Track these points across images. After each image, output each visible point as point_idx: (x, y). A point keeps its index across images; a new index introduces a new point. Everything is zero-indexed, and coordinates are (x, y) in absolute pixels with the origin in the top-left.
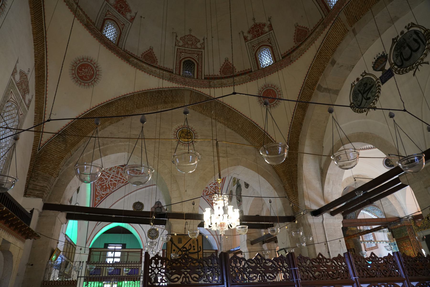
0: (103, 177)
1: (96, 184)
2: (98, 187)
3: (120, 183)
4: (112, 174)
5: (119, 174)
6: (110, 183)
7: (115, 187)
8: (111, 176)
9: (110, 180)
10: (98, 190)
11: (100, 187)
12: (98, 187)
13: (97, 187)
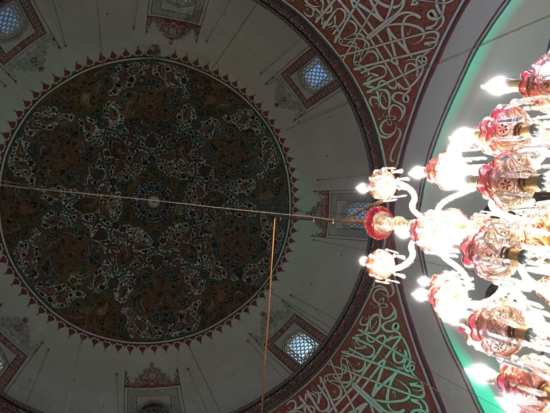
0: (404, 47)
1: (438, 34)
4: (370, 36)
5: (345, 22)
6: (391, 7)
8: (376, 32)
9: (384, 17)
10: (444, 7)
11: (431, 15)
12: (436, 19)
13: (441, 20)
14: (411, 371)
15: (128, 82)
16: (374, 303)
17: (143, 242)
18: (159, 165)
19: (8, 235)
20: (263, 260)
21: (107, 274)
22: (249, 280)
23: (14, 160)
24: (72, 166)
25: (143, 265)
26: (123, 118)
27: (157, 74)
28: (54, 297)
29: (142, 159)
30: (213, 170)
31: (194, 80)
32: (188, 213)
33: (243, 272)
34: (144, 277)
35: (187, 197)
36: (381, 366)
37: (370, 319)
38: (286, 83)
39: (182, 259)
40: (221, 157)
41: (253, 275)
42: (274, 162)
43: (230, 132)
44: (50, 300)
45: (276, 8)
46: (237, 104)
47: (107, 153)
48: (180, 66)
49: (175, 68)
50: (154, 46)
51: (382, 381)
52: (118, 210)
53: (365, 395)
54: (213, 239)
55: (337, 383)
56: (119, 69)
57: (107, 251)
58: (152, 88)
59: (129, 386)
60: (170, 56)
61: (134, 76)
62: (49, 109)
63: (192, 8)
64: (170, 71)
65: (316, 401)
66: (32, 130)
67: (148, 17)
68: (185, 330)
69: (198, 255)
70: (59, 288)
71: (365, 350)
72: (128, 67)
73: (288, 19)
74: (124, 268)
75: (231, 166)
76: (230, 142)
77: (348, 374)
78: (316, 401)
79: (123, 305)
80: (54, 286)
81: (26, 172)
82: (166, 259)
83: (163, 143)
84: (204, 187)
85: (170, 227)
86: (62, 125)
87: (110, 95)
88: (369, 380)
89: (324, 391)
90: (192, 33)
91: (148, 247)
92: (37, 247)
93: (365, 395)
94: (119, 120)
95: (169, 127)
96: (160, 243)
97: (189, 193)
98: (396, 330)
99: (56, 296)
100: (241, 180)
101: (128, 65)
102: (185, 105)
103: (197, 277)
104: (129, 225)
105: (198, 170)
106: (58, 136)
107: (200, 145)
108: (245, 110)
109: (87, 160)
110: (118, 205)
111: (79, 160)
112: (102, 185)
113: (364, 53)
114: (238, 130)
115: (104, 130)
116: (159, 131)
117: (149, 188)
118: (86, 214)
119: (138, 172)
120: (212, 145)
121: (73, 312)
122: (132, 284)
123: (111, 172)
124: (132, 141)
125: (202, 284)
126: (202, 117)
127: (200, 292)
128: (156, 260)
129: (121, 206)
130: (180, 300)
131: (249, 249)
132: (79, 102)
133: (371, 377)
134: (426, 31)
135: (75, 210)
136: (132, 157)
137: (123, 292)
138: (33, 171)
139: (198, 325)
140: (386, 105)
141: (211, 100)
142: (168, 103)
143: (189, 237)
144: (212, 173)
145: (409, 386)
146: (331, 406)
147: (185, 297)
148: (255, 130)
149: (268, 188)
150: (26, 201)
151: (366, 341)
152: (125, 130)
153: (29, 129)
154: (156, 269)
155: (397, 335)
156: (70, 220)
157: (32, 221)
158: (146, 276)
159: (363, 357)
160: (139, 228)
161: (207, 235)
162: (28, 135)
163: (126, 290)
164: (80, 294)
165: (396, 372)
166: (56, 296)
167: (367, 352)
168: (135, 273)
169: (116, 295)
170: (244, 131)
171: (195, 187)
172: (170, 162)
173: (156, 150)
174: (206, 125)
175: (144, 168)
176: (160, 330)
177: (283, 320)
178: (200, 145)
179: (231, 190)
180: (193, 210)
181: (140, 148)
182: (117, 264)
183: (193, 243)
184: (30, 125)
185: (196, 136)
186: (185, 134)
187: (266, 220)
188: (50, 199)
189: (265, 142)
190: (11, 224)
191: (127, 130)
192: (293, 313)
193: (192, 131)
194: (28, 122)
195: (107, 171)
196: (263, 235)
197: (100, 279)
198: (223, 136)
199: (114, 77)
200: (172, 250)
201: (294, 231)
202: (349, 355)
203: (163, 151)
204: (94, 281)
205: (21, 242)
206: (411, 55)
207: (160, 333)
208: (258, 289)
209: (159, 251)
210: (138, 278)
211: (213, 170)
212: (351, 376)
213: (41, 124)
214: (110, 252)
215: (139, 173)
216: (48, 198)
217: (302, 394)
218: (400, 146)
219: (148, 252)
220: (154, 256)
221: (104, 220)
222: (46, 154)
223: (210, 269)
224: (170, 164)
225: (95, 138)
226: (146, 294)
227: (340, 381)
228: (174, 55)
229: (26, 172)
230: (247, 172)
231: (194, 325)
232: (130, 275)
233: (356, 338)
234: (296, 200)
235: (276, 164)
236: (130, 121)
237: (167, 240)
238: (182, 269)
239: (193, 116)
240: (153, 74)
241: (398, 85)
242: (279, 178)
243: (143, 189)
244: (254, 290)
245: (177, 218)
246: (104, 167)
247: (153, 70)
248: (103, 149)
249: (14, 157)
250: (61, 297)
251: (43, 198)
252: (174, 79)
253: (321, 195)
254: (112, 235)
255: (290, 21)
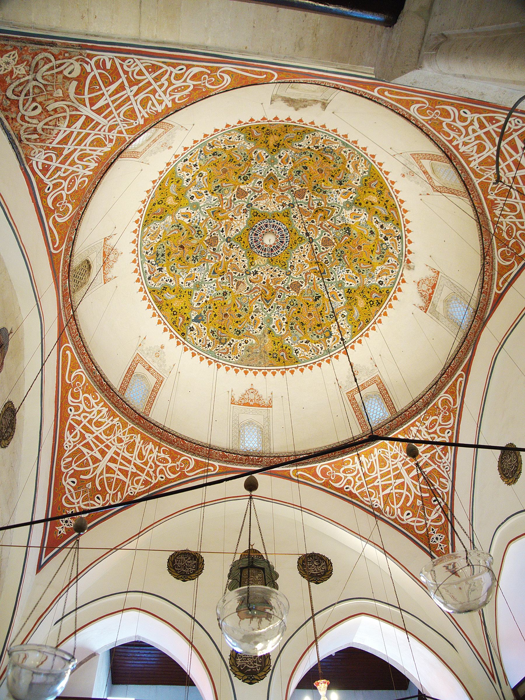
1: (393, 517)
2: (405, 517)
3: (441, 458)
7: (444, 477)
9: (412, 478)
10: (412, 524)
11: (408, 514)
13: (403, 520)
14: (129, 492)
15: (384, 235)
16: (180, 458)
17: (232, 229)
18: (304, 246)
19: (250, 128)
20: (210, 341)
21: (204, 200)
22: (192, 329)
23: (321, 137)
24: (311, 176)
25: (210, 229)
26: (351, 223)
27: (389, 261)
28: (187, 163)
29: (311, 232)
30: (296, 295)
31: (380, 292)
32: (257, 269)
33: (199, 322)
34: (198, 231)
35: (272, 268)
36: (131, 468)
37: (167, 457)
38: (370, 378)
39: (213, 264)
40: (308, 304)
41: (196, 332)
42: (300, 355)
43: (331, 315)
44: (187, 160)
45: (433, 390)
46: (355, 327)
47: (320, 204)
48: (394, 283)
49: (393, 279)
50: (414, 266)
51: (120, 470)
52: (264, 208)
53: (108, 457)
54: (230, 292)
55: (115, 433)
56: (397, 231)
57: (226, 199)
58: (377, 253)
59: (105, 241)
60: (403, 277)
61: (388, 241)
62: (365, 169)
63: (441, 312)
64: (391, 273)
65: (101, 417)
66: (348, 153)
67: (439, 272)
68: (149, 274)
69: (216, 279)
70: (195, 165)
71: (142, 455)
72: (398, 239)
73: (422, 397)
74: (209, 214)
75: (299, 312)
76: (321, 314)
77: (123, 441)
78: (101, 417)
79: (173, 216)
80: (198, 161)
81: (309, 143)
82: (214, 249)
83: (325, 252)
84: (280, 285)
85: (244, 252)
86: (350, 175)
87: (373, 218)
88: (119, 459)
89: (108, 423)
90: (423, 304)
91: (226, 233)
92: (236, 147)
93: (108, 457)
94: (350, 219)
95: (340, 260)
96: (229, 244)
97: (275, 271)
98: (159, 478)
99: (188, 164)
100: (285, 321)
101: (400, 240)
102: (358, 278)
103: (196, 279)
104: (248, 217)
105: (297, 280)
106: (339, 170)
107: (321, 285)
108: (350, 333)
109: (315, 187)
110: (269, 208)
111: (315, 181)
112: (290, 197)
113: (387, 458)
114: (332, 323)
115: (342, 205)
116: (336, 250)
117: (283, 235)
118: (263, 182)
119: (300, 227)
120: (320, 297)
121: (172, 179)
122: (193, 222)
123: (301, 205)
124: (329, 226)
125: (189, 284)
126: (346, 291)
127: (182, 283)
128: (213, 241)
129: (267, 211)
130: (175, 266)
131: (220, 327)
132: (369, 192)
133: (122, 461)
134: (397, 509)
135: (268, 174)
136: (313, 224)
137: (185, 216)
138: (309, 148)
139: (153, 286)
140: (344, 472)
141: (362, 303)
142: (362, 264)
143: (233, 269)
144: (293, 293)
145: (118, 491)
146: (97, 431)
147: (177, 270)
148: (331, 339)
149: (277, 346)
150: (281, 140)
151: (150, 453)
152: (340, 222)
153: (349, 152)
154: (206, 241)
155: (155, 479)
156: (258, 170)
157: (261, 143)
158: (200, 233)
159: (136, 453)
160: (245, 225)
161: (235, 286)
162: (344, 150)
163: (187, 218)
164: (188, 182)
165: (127, 481)
166: (188, 164)
167: (141, 456)
168: (202, 224)
169: (184, 210)
170: (330, 329)
171: (281, 277)
172: (307, 256)
173: (319, 245)
174: (338, 294)
175: (303, 233)
176: (150, 253)
177: (158, 368)
178: (321, 285)
179: (276, 310)
180: (259, 273)
181: (322, 232)
182: (212, 207)
183: (227, 274)
184: (354, 153)
185: (329, 283)
186: (332, 273)
187: (246, 343)
188: (280, 157)
189: (319, 348)
190: (261, 129)
191: (340, 224)
192: (164, 377)
193: (335, 280)
194: (356, 153)
195: (302, 202)
196: (233, 341)
197: (200, 194)
198: (327, 308)
199: (389, 225)
200: (222, 254)
201: (237, 371)
202: (137, 441)
203: (317, 251)
204: (199, 190)
205: (242, 136)
206: (381, 496)
207: (147, 253)
208: (184, 338)
209: (222, 242)
210: (198, 226)
211: (296, 295)
212: (121, 444)
213: (352, 161)
214: (224, 201)
215: (298, 228)
216: (282, 155)
217: (105, 405)
218: (310, 481)
219: (221, 233)
220: (217, 239)
221: (255, 197)
222: (324, 158)
223: (202, 290)
224: (304, 256)
225: (335, 197)
226: (183, 235)
227: (116, 436)
228: (403, 281)
229: (309, 143)
230: (292, 327)
231: (153, 283)
232: (201, 219)
233: (151, 446)
234: (265, 374)
235: (298, 356)
236: (348, 228)
237: (232, 249)
238: (204, 265)
239: (348, 284)
240: (389, 258)
241: (359, 483)
242: (285, 359)
243: (283, 230)
244: (183, 334)
245: (252, 258)
246: (307, 200)
247: (393, 259)
248: (323, 201)
249: (324, 138)
250: (187, 168)
251: (282, 152)
252: (383, 275)
253: (269, 399)
254: (241, 203)
255: (420, 399)
